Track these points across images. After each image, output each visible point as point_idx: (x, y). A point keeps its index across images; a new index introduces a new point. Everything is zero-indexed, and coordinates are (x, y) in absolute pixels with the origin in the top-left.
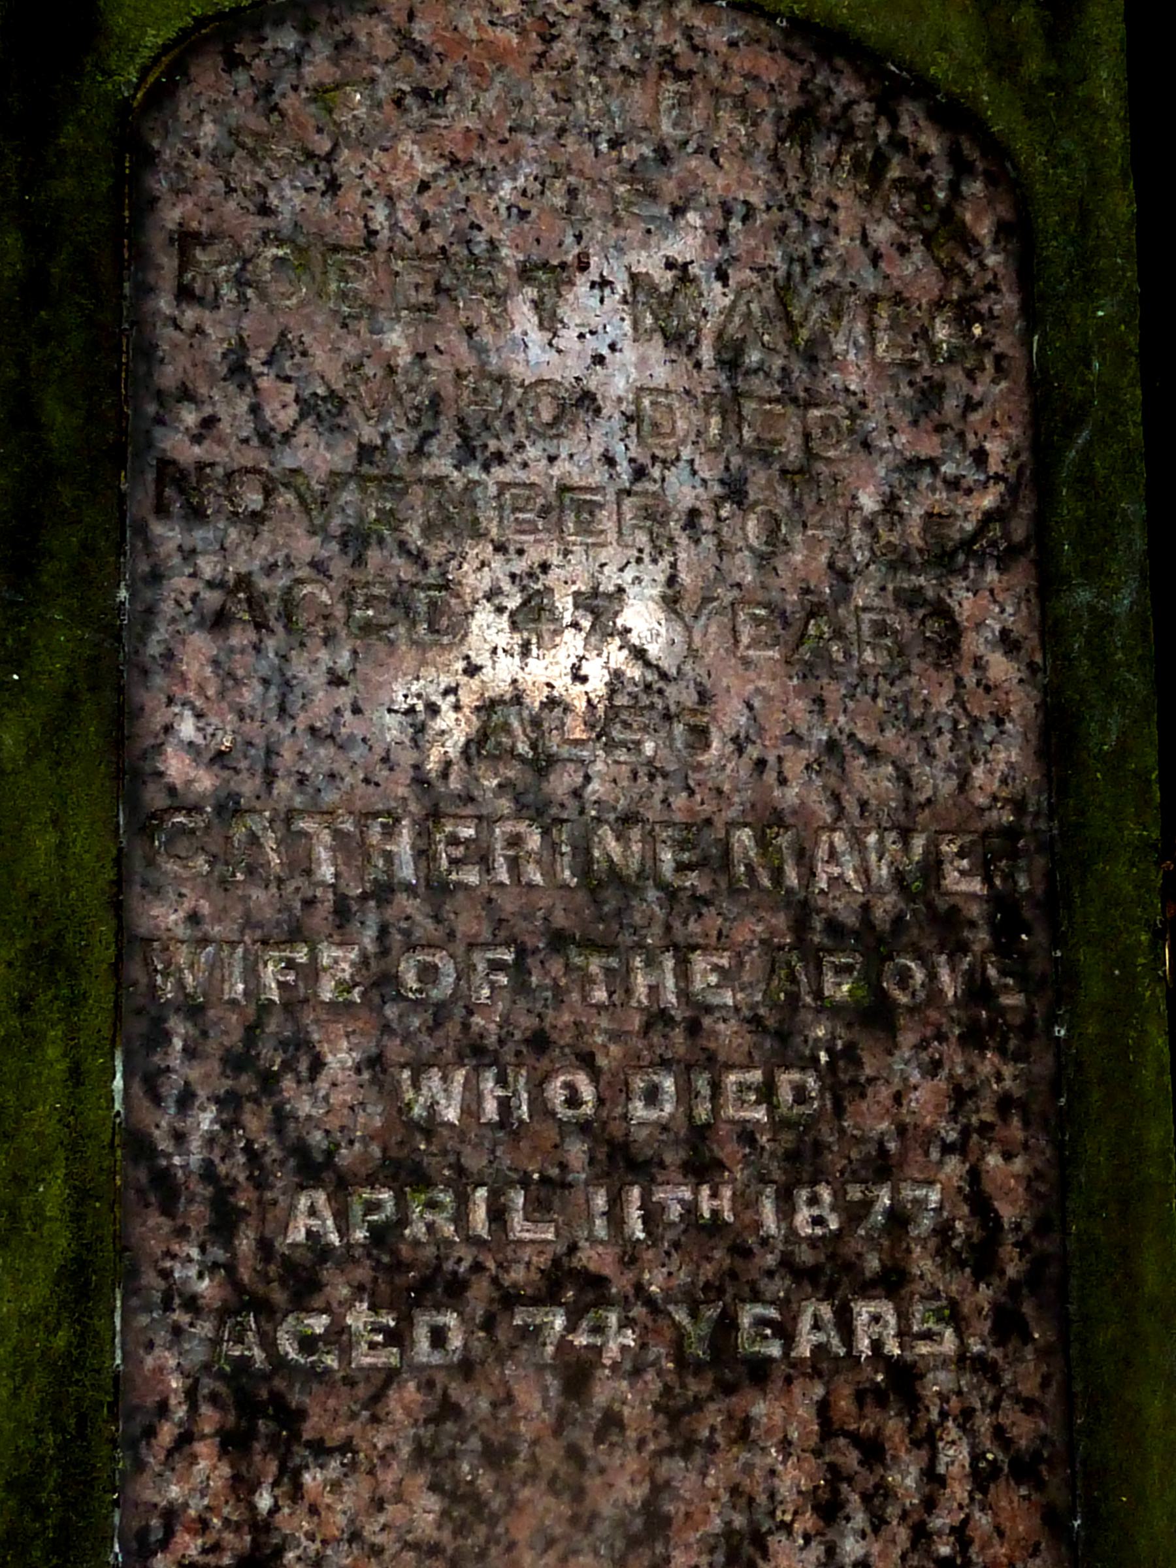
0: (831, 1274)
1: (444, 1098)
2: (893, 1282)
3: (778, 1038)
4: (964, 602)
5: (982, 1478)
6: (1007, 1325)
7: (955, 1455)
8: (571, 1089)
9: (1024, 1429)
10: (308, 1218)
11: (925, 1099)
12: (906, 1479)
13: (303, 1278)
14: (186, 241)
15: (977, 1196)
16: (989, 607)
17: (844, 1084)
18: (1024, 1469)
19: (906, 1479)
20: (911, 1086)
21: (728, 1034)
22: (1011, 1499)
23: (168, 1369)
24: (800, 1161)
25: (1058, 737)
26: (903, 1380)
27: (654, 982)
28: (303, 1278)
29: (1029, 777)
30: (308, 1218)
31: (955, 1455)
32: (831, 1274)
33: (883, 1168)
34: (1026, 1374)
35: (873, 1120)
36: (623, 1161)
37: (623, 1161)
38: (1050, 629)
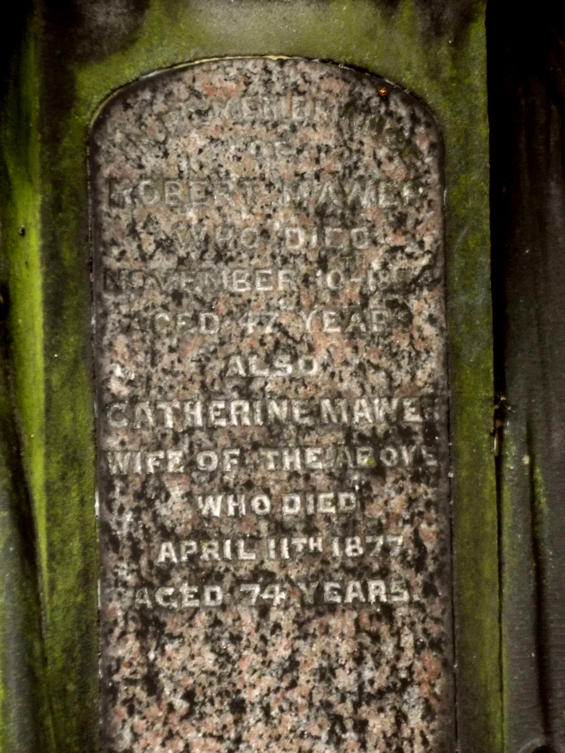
0: (360, 570)
1: (213, 506)
2: (384, 574)
3: (339, 480)
4: (414, 304)
5: (418, 648)
6: (428, 590)
7: (408, 640)
8: (261, 502)
9: (435, 630)
10: (166, 552)
11: (397, 503)
12: (388, 648)
13: (164, 575)
14: (112, 181)
15: (418, 542)
16: (424, 305)
17: (365, 497)
18: (435, 645)
19: (388, 648)
20: (391, 498)
21: (320, 480)
22: (429, 656)
23: (117, 608)
24: (348, 527)
25: (451, 357)
26: (387, 611)
27: (292, 460)
28: (164, 575)
29: (440, 374)
30: (166, 552)
31: (408, 640)
32: (360, 570)
33: (380, 529)
34: (436, 608)
35: (376, 511)
36: (280, 529)
37: (280, 529)
38: (449, 313)
